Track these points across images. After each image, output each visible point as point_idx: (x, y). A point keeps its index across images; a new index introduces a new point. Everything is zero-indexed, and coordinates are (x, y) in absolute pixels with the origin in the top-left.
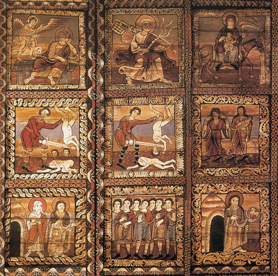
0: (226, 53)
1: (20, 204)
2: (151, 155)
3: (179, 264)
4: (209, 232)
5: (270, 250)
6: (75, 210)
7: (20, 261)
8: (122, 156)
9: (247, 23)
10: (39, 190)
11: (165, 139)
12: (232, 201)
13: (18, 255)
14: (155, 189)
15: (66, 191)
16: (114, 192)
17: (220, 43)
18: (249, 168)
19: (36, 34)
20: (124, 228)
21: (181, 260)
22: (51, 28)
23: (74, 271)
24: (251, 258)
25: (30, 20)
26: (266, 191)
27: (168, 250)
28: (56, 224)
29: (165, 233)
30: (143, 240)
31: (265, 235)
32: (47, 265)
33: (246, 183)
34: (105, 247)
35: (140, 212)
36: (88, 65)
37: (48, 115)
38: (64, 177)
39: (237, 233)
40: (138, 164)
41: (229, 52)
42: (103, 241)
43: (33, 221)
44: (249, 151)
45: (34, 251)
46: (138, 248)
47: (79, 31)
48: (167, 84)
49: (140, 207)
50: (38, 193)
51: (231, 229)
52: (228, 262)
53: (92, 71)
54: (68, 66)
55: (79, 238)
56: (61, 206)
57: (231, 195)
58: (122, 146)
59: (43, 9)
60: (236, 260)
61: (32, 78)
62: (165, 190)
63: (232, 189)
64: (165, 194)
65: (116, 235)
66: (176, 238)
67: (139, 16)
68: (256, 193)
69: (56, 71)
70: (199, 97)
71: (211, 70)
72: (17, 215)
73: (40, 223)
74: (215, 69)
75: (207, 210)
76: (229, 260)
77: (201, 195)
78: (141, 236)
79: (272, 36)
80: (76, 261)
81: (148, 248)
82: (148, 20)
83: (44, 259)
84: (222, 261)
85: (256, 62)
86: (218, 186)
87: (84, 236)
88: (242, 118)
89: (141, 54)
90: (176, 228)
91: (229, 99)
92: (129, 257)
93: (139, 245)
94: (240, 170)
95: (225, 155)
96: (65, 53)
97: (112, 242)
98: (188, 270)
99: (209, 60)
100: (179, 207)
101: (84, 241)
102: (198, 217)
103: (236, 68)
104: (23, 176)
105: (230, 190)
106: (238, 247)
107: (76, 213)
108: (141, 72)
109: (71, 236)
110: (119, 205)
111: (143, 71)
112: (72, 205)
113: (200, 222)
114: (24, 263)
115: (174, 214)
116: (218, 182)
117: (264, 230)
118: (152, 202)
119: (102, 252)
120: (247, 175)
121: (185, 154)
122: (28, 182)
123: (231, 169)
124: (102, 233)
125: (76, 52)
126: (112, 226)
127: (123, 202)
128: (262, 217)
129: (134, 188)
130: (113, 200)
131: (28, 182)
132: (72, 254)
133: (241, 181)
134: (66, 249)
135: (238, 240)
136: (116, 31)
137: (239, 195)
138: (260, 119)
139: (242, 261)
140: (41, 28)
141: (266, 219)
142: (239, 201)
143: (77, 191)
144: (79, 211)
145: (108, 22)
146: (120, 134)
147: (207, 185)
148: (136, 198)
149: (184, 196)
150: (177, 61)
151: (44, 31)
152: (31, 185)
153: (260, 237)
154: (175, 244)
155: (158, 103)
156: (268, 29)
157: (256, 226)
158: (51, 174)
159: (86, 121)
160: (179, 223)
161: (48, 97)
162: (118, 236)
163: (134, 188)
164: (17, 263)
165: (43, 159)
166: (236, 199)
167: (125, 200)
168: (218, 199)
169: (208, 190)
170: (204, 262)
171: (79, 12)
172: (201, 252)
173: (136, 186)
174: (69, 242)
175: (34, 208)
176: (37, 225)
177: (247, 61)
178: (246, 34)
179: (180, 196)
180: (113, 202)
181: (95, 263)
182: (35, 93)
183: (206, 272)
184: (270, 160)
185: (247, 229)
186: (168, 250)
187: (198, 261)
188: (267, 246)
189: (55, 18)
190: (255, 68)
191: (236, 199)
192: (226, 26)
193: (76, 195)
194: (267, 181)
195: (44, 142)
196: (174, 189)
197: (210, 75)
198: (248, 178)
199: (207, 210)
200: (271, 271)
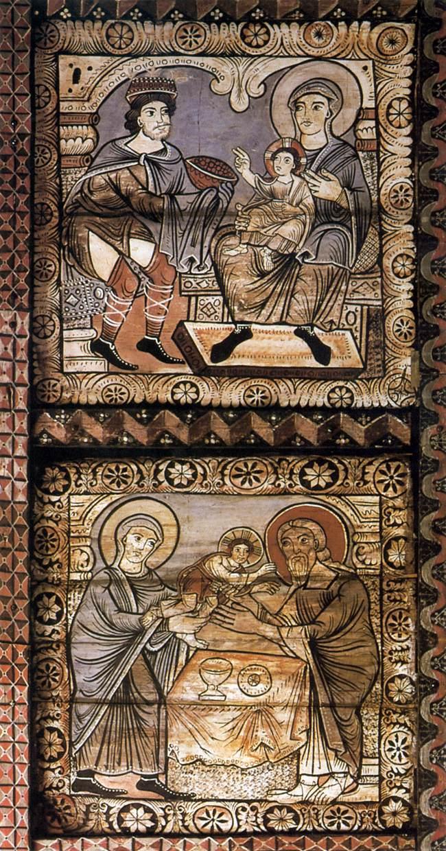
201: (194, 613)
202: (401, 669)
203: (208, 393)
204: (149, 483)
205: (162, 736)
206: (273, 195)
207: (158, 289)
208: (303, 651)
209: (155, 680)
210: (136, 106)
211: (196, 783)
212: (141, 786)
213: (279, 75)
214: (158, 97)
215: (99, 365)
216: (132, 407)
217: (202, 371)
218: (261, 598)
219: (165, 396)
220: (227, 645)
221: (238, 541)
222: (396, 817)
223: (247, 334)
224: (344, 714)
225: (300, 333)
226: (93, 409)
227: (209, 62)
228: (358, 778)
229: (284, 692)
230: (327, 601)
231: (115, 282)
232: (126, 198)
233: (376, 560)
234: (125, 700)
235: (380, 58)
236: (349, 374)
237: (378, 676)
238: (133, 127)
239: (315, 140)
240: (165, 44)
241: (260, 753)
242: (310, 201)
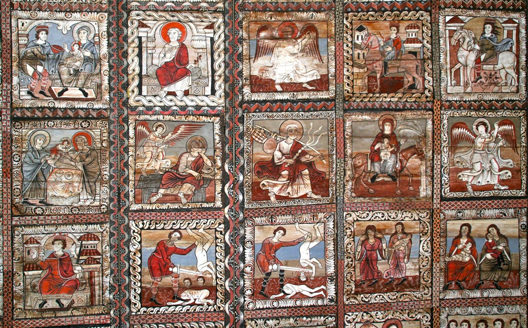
0: (382, 162)
2: (297, 281)
8: (265, 283)
9: (406, 127)
11: (313, 263)
14: (303, 321)
15: (200, 325)
17: (376, 151)
18: (408, 293)
19: (164, 143)
22: (181, 136)
25: (157, 128)
26: (427, 318)
36: (225, 179)
37: (179, 239)
38: (198, 309)
40: (284, 292)
41: (385, 161)
44: (408, 274)
47: (214, 139)
48: (316, 199)
53: (230, 186)
54: (202, 181)
57: (388, 323)
58: (264, 272)
59: (173, 114)
61: (159, 196)
62: (315, 321)
63: (390, 317)
64: (315, 326)
67: (283, 121)
68: (416, 320)
69: (187, 188)
70: (353, 214)
71: (366, 182)
74: (370, 181)
77: (355, 325)
79: (433, 142)
82: (294, 125)
85: (416, 172)
86: (373, 313)
88: (400, 236)
89: (286, 166)
91: (386, 214)
94: (398, 295)
95: (382, 278)
96: (198, 165)
99: (364, 171)
103: (394, 180)
104: (151, 309)
105: (387, 318)
108: (284, 187)
111: (288, 185)
120: (406, 300)
121: (337, 279)
123: (388, 294)
125: (210, 165)
129: (279, 320)
133: (399, 308)
136: (257, 139)
138: (421, 237)
140: (169, 137)
143: (214, 325)
145: (247, 129)
146: (262, 258)
150: (327, 173)
151: (173, 140)
155: (306, 222)
156: (430, 134)
158: (183, 306)
159: (223, 245)
161: (178, 218)
163: (279, 320)
165: (174, 289)
169: (363, 318)
171: (213, 117)
173: (282, 317)
177: (405, 172)
178: (405, 140)
182: (163, 213)
184: (432, 283)
189: (187, 125)
190: (414, 179)
192: (383, 130)
194: (428, 306)
195: (175, 270)
196: (325, 320)
197: (365, 187)
198: (407, 304)
201: (54, 159)
202: (105, 173)
203: (58, 105)
204: (42, 126)
205: (45, 190)
206: (73, 55)
207: (44, 78)
208: (81, 168)
209: (44, 176)
210: (38, 32)
211: (54, 201)
212: (40, 202)
213: (75, 25)
214: (44, 30)
215: (29, 97)
216: (38, 108)
217: (56, 99)
218: (71, 155)
219: (46, 105)
220: (62, 167)
221: (65, 141)
222: (104, 209)
223: (67, 90)
224: (92, 184)
225: (80, 89)
226: (27, 109)
227: (57, 22)
228: (94, 200)
229: (76, 179)
230: (87, 156)
231: (34, 76)
232: (36, 55)
233: (99, 145)
234: (36, 180)
235: (100, 21)
236: (92, 100)
237: (100, 174)
238: (38, 38)
239: (84, 42)
240: (46, 17)
241: (70, 194)
242: (82, 57)
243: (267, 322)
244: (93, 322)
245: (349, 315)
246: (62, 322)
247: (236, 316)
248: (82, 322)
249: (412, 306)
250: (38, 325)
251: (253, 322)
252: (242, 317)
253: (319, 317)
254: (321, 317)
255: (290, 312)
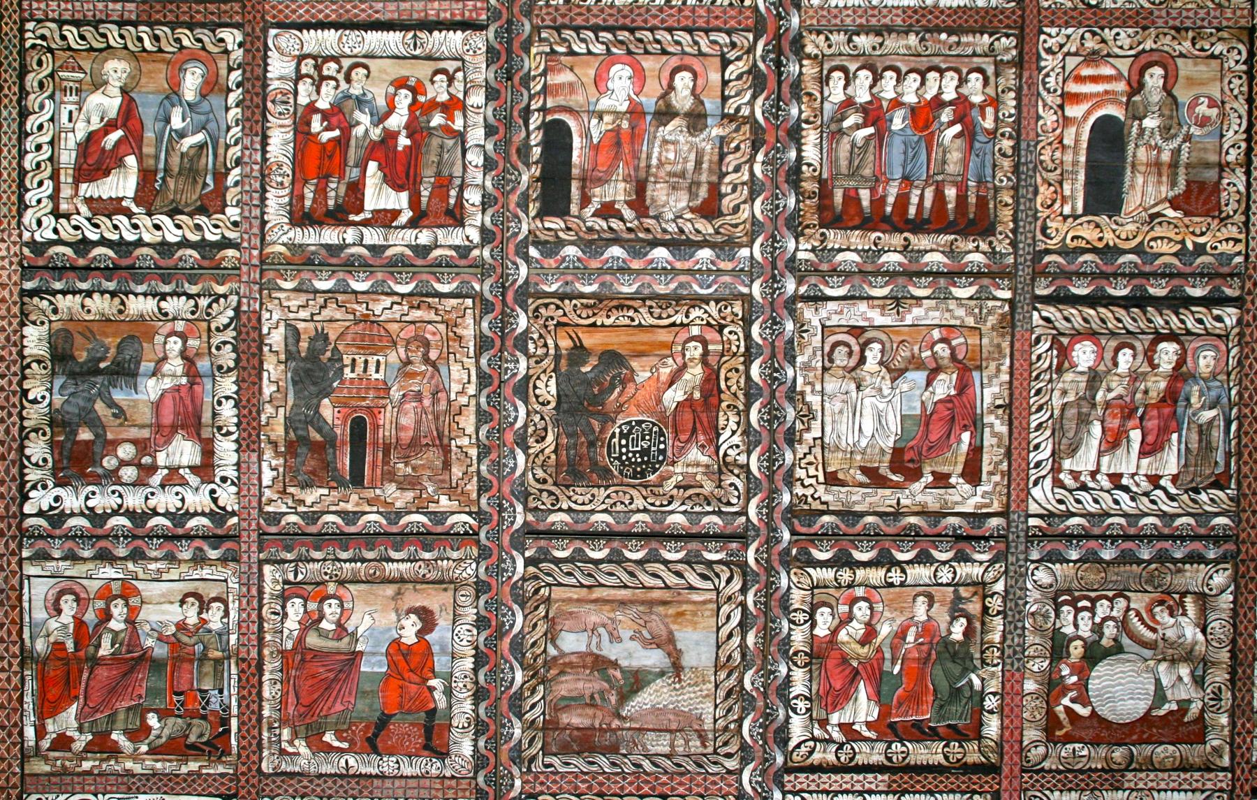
1: (571, 70)
3: (1003, 247)
4: (1083, 159)
5: (1246, 212)
6: (723, 92)
7: (569, 229)
10: (623, 35)
12: (1147, 77)
13: (564, 212)
14: (940, 42)
15: (697, 38)
16: (830, 46)
20: (853, 145)
21: (1007, 236)
23: (718, 257)
24: (1193, 233)
26: (1240, 53)
27: (972, 209)
28: (670, 127)
29: (965, 163)
30: (907, 179)
31: (1233, 171)
32: (643, 240)
33: (1187, 29)
34: (799, 193)
35: (896, 103)
39: (1158, 164)
42: (794, 175)
43: (607, 118)
45: (608, 199)
46: (891, 200)
49: (899, 89)
50: (622, 42)
51: (1142, 154)
52: (1133, 243)
55: (730, 169)
56: (683, 81)
57: (1144, 59)
60: (1155, 239)
62: (968, 44)
63: (1149, 45)
65: (833, 162)
66: (994, 177)
68: (1213, 56)
72: (563, 103)
73: (625, 125)
75: (1076, 98)
76: (1135, 237)
77: (1064, 59)
78: (901, 170)
80: (722, 230)
81: (921, 199)
83: (636, 222)
84: (1117, 241)
86: (1108, 34)
87: (746, 162)
90: (997, 148)
92: (867, 224)
93: (892, 192)
97: (820, 181)
98: (1026, 260)
100: (1003, 92)
101: (746, 177)
102: (1055, 118)
105: (1141, 47)
106: (1161, 202)
107: (725, 99)
109: (711, 162)
110: (842, 82)
112: (715, 77)
113: (1059, 131)
114: (582, 234)
115: (990, 111)
116: (1110, 22)
117: (1231, 158)
118: (932, 76)
119: (792, 206)
120: (1189, 6)
122: (595, 11)
124: (793, 154)
126: (821, 137)
127: (854, 74)
128: (1226, 123)
129: (882, 36)
130: (826, 67)
131: (595, 11)
132: (710, 210)
133: (1171, 23)
134: (697, 195)
135: (1160, 182)
137: (1167, 63)
139: (1170, 240)
141: (1237, 128)
142: (1165, 77)
143: (728, 41)
144: (733, 93)
147: (1081, 31)
148: (888, 63)
149: (1019, 63)
152: (605, 21)
153: (1221, 178)
154: (992, 191)
157: (1208, 146)
160: (1003, 135)
162: (838, 167)
164: (561, 234)
166: (1158, 71)
167: (858, 69)
168: (1108, 71)
170: (1068, 241)
172: (1061, 214)
173: (890, 29)
174: (704, 177)
175: (610, 85)
176: (617, 130)
179: (1008, 62)
180: (825, 72)
181: (773, 237)
183: (1073, 268)
185: (1184, 156)
186: (972, 209)
187: (1051, 239)
188: (1238, 202)
191: (1158, 71)
193: (726, 50)
194: (1243, 22)
196: (992, 44)
199: (1076, 98)
200: (1247, 269)
243: (855, 38)
244: (448, 15)
245: (1050, 35)
246: (377, 12)
247: (781, 18)
248: (423, 14)
249: (1203, 20)
250: (321, 16)
251: (822, 37)
252: (795, 21)
253: (978, 35)
254: (982, 34)
255: (910, 17)
